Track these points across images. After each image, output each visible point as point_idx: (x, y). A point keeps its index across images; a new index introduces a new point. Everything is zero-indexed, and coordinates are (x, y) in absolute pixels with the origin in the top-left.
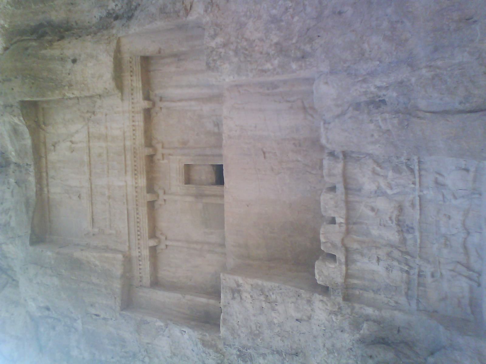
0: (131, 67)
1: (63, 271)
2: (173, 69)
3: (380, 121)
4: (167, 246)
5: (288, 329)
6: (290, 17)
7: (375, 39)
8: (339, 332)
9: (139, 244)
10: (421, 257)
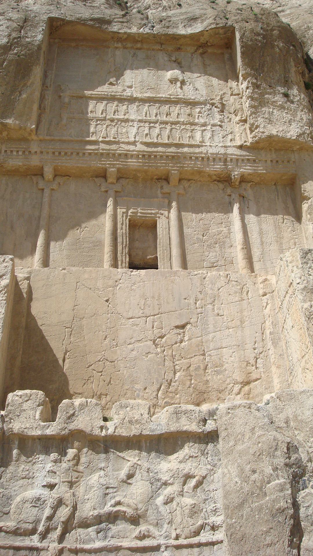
1: (15, 51)
3: (277, 481)
4: (43, 190)
9: (48, 153)
10: (61, 551)
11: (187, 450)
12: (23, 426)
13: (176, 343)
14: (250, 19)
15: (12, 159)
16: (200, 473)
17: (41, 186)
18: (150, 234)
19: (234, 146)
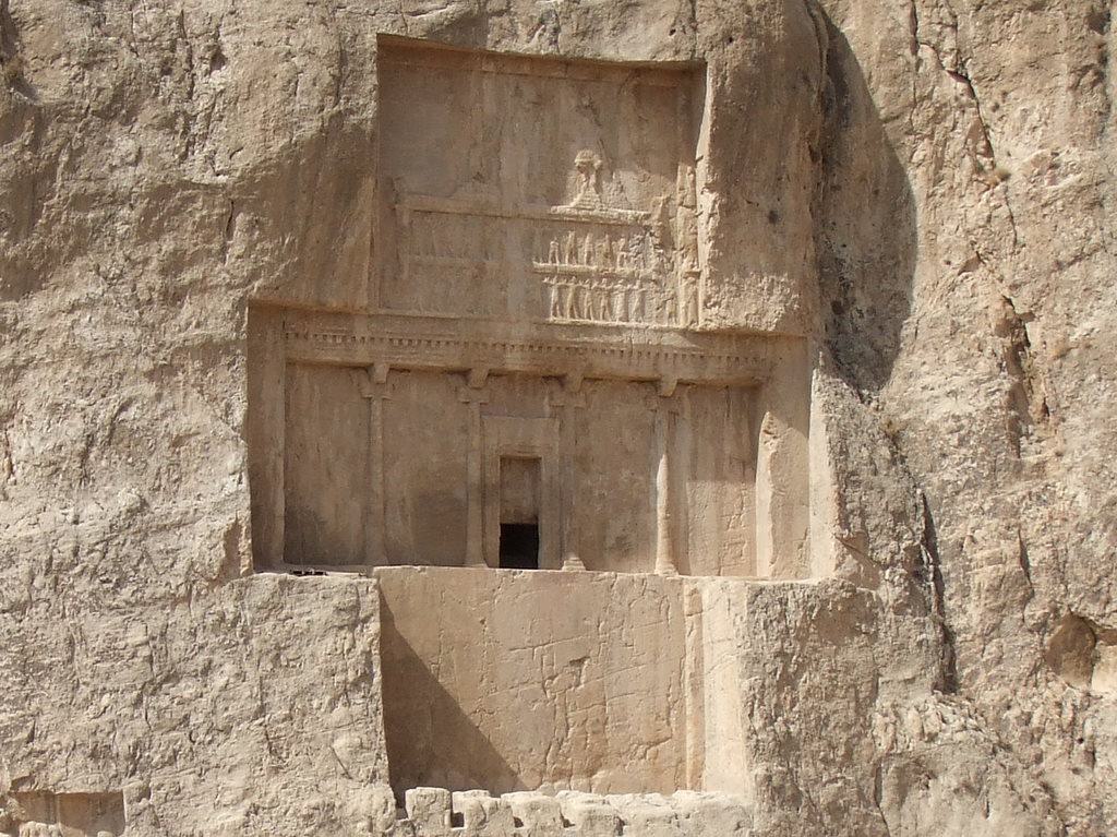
13: (570, 687)
14: (736, 29)
17: (367, 391)
18: (527, 473)
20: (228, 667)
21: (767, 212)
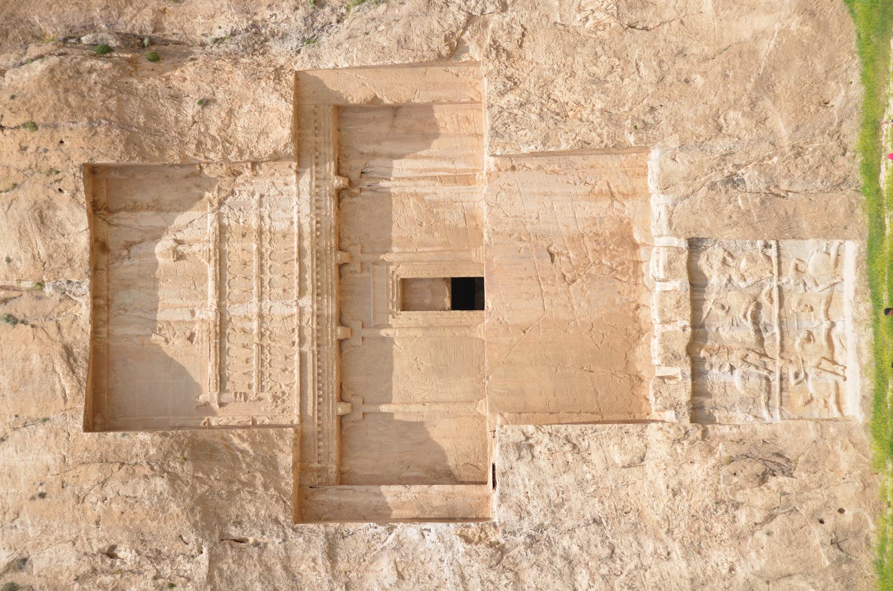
0: (316, 121)
1: (178, 465)
2: (384, 128)
3: (740, 202)
5: (609, 483)
6: (618, 79)
7: (732, 114)
8: (685, 466)
10: (782, 358)
11: (702, 262)
12: (684, 393)
13: (570, 262)
15: (329, 453)
16: (722, 253)
17: (359, 416)
19: (297, 182)
20: (566, 542)
21: (199, 107)
